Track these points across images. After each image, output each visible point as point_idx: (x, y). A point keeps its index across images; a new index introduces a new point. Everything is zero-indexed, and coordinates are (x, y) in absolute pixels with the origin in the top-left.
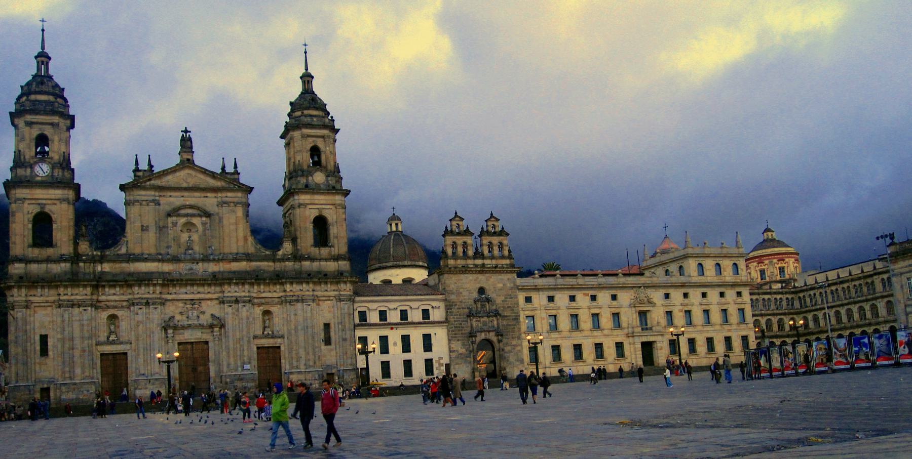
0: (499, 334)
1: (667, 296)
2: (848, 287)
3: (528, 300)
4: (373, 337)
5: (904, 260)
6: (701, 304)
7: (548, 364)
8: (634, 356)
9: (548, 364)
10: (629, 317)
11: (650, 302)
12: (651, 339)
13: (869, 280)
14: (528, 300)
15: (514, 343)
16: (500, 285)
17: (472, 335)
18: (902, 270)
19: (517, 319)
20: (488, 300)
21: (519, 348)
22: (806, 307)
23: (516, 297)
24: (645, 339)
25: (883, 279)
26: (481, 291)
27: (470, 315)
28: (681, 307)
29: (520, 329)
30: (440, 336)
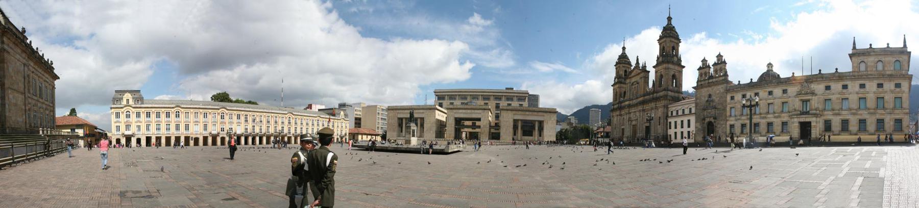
0: (715, 118)
1: (828, 88)
3: (732, 98)
4: (672, 120)
6: (857, 93)
7: (738, 134)
8: (796, 132)
9: (738, 134)
10: (797, 104)
11: (813, 93)
12: (808, 120)
14: (732, 98)
17: (704, 119)
19: (725, 109)
20: (713, 101)
24: (802, 120)
26: (710, 96)
27: (704, 110)
30: (693, 119)
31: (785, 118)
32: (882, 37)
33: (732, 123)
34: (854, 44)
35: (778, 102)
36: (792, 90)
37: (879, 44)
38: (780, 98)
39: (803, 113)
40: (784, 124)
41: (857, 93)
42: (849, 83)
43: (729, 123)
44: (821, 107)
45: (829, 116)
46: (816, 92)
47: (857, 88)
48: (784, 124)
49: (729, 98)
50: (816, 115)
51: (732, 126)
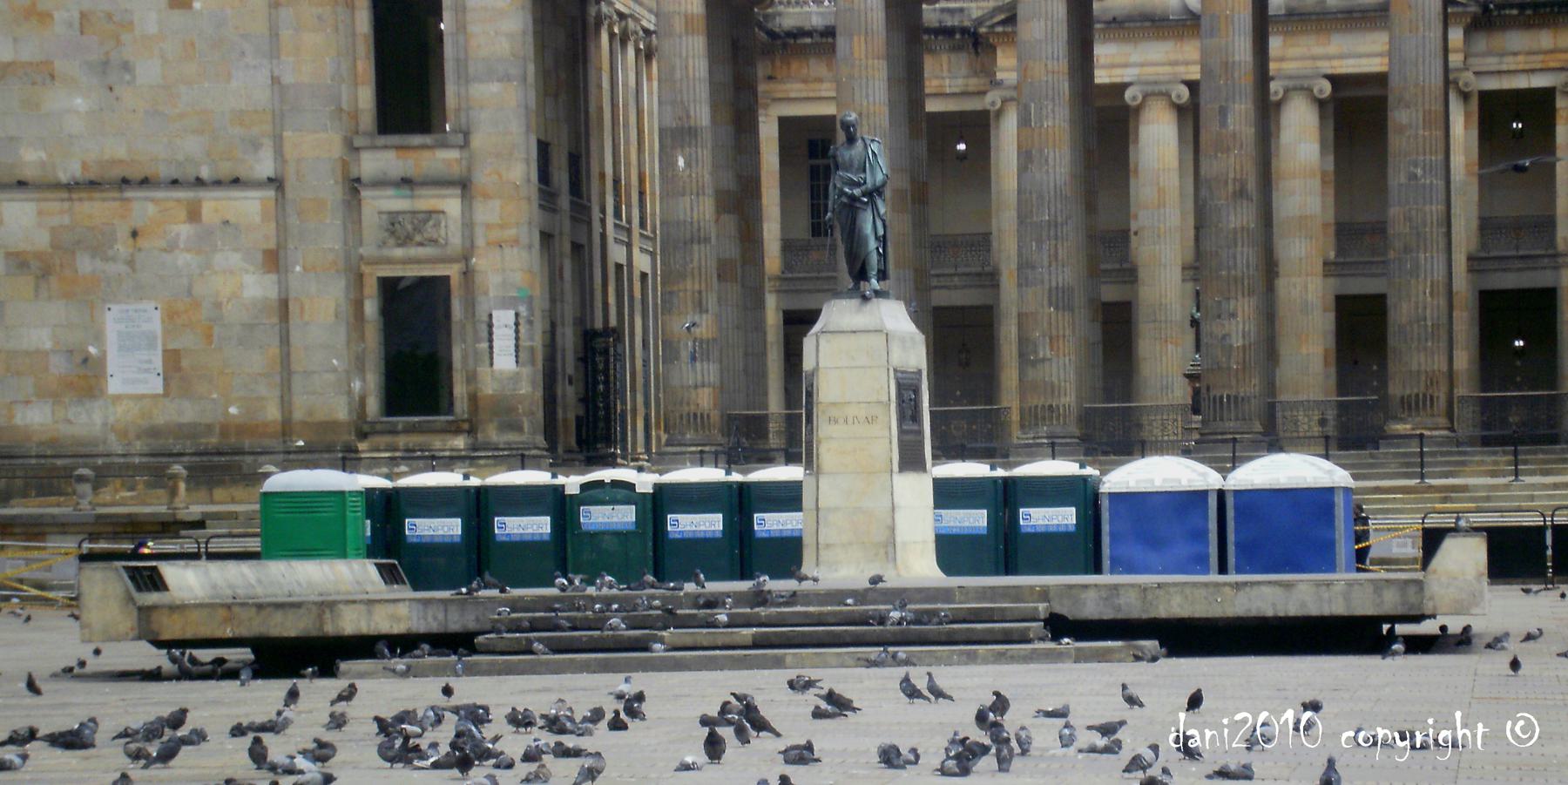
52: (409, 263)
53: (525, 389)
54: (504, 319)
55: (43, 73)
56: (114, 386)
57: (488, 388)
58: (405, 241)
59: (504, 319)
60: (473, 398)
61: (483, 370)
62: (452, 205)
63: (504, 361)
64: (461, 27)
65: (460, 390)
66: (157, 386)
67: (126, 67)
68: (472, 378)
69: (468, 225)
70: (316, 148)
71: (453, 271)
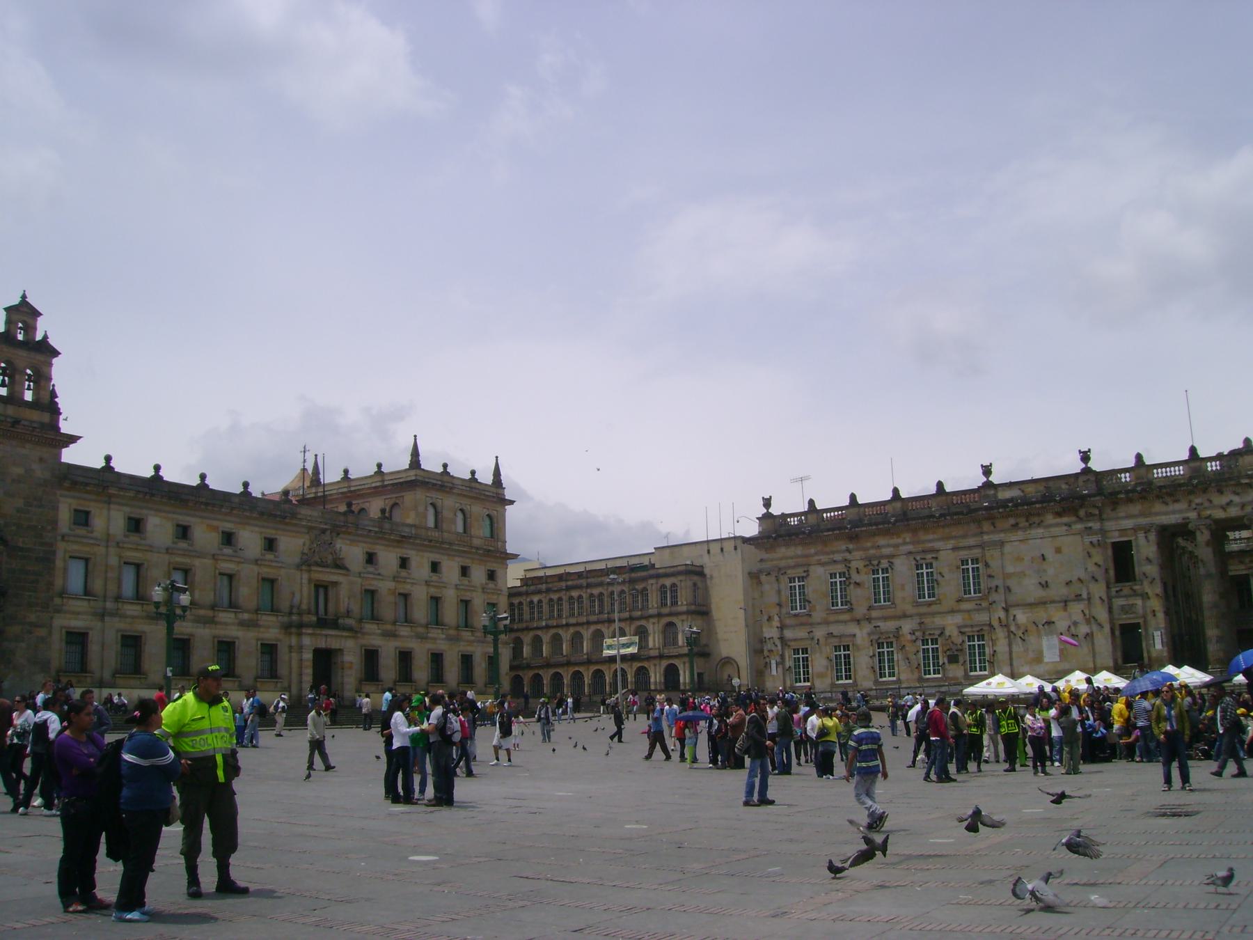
2: (521, 603)
5: (787, 545)
11: (339, 565)
12: (334, 644)
13: (639, 587)
14: (82, 518)
15: (32, 617)
16: (18, 471)
18: (783, 563)
19: (48, 559)
21: (42, 632)
22: (521, 620)
23: (56, 509)
24: (322, 644)
25: (663, 586)
28: (391, 585)
29: (50, 584)
31: (271, 630)
32: (459, 451)
33: (77, 624)
34: (415, 453)
35: (249, 575)
36: (292, 544)
37: (460, 471)
38: (256, 562)
39: (323, 623)
40: (269, 650)
41: (427, 583)
42: (411, 553)
43: (63, 622)
44: (355, 608)
45: (373, 637)
46: (348, 563)
47: (426, 569)
48: (269, 650)
49: (64, 515)
50: (354, 632)
51: (78, 639)
52: (1126, 619)
53: (1165, 654)
54: (1157, 634)
55: (1022, 574)
56: (1046, 660)
57: (1154, 655)
58: (1127, 613)
59: (1157, 634)
60: (1150, 658)
61: (1152, 649)
62: (1139, 602)
63: (1158, 646)
64: (1138, 551)
65: (1145, 655)
66: (1058, 659)
67: (1045, 571)
68: (1149, 652)
69: (1144, 607)
70: (1099, 590)
71: (1141, 621)
